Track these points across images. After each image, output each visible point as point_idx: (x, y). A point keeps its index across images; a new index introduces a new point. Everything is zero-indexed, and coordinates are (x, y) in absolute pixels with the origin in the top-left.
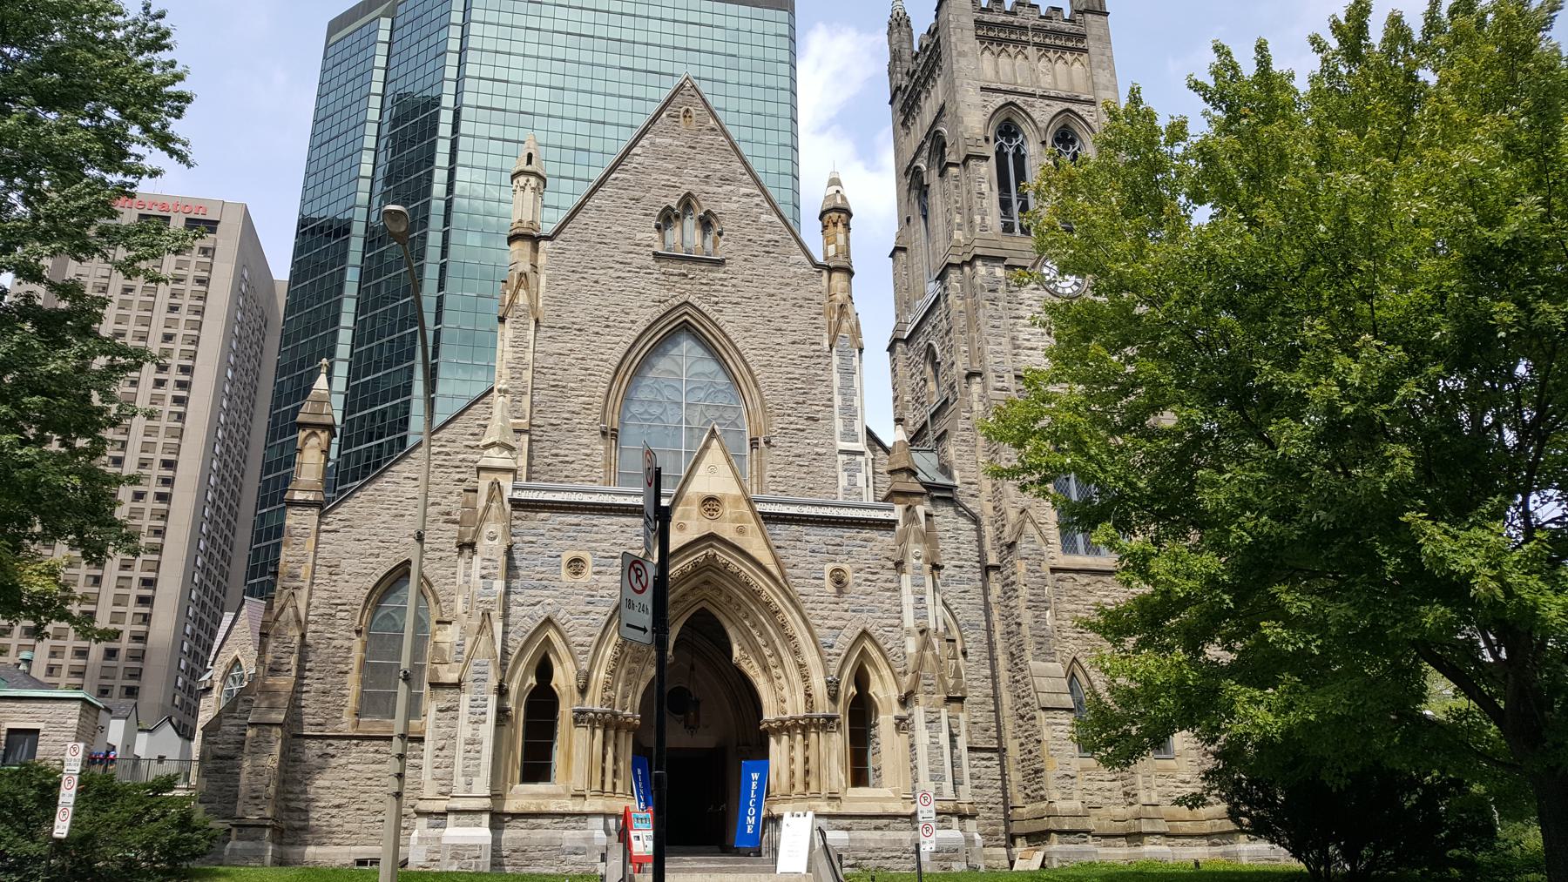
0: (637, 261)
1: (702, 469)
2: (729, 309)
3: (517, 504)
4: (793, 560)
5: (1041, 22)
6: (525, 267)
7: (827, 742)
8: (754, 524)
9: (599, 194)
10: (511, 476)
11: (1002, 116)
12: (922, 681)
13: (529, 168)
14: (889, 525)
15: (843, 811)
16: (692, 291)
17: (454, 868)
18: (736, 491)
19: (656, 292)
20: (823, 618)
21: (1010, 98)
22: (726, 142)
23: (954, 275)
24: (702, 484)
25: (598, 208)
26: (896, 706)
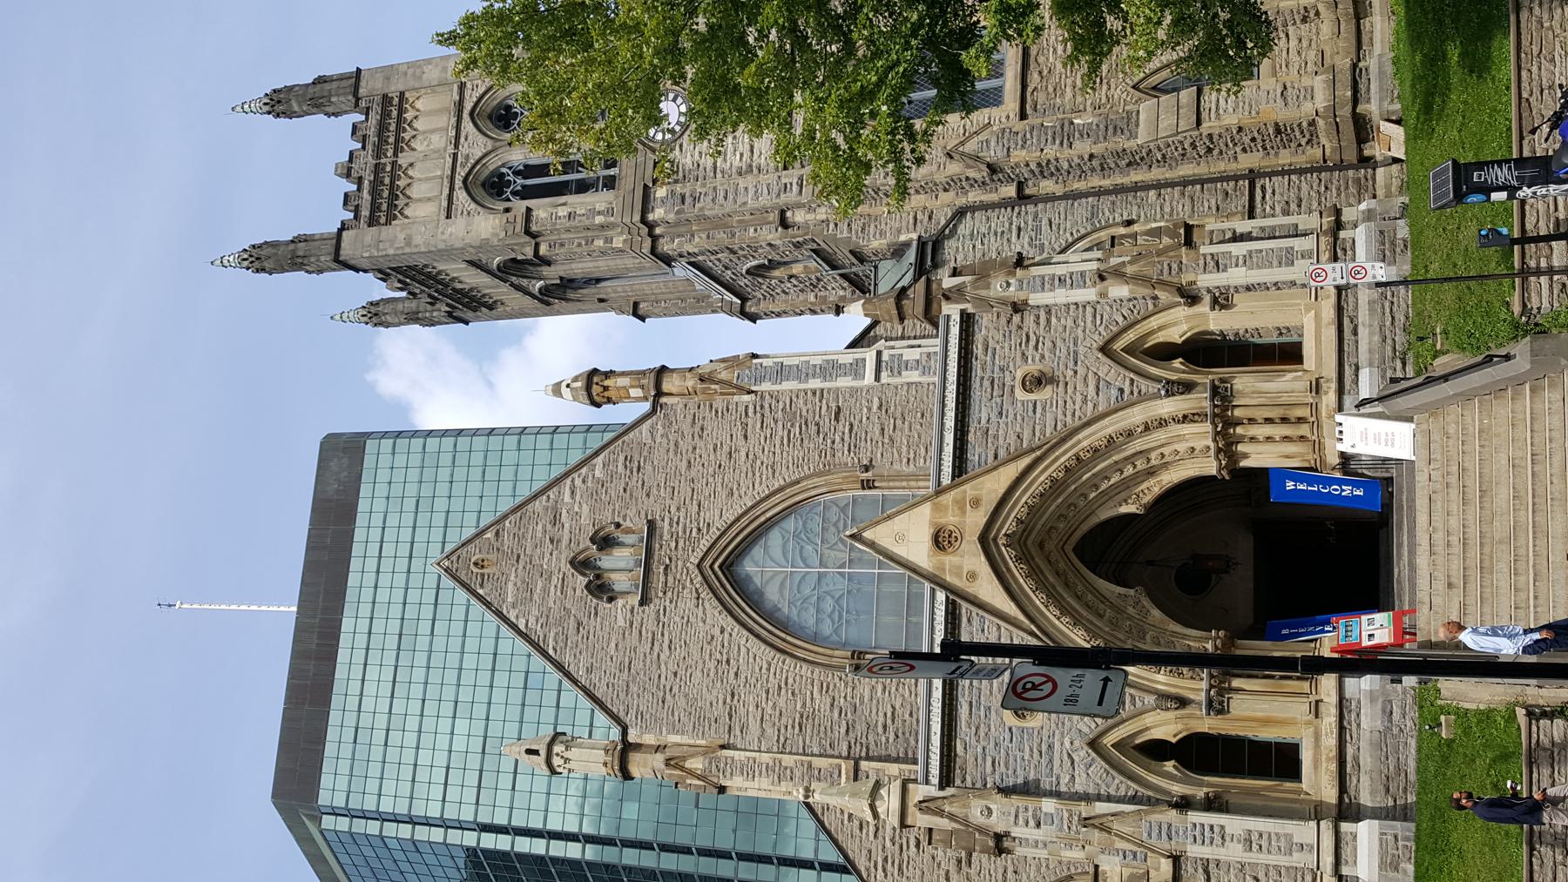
0: (650, 625)
1: (900, 551)
2: (707, 515)
3: (946, 780)
4: (1012, 439)
5: (370, 147)
6: (659, 759)
7: (1243, 394)
8: (967, 487)
9: (572, 669)
10: (911, 786)
11: (479, 193)
12: (1165, 277)
13: (543, 753)
14: (967, 320)
15: (1334, 375)
16: (685, 559)
17: (1411, 868)
18: (926, 508)
19: (687, 603)
20: (1085, 401)
21: (458, 183)
22: (512, 518)
23: (666, 247)
24: (919, 552)
25: (589, 670)
26: (1197, 309)
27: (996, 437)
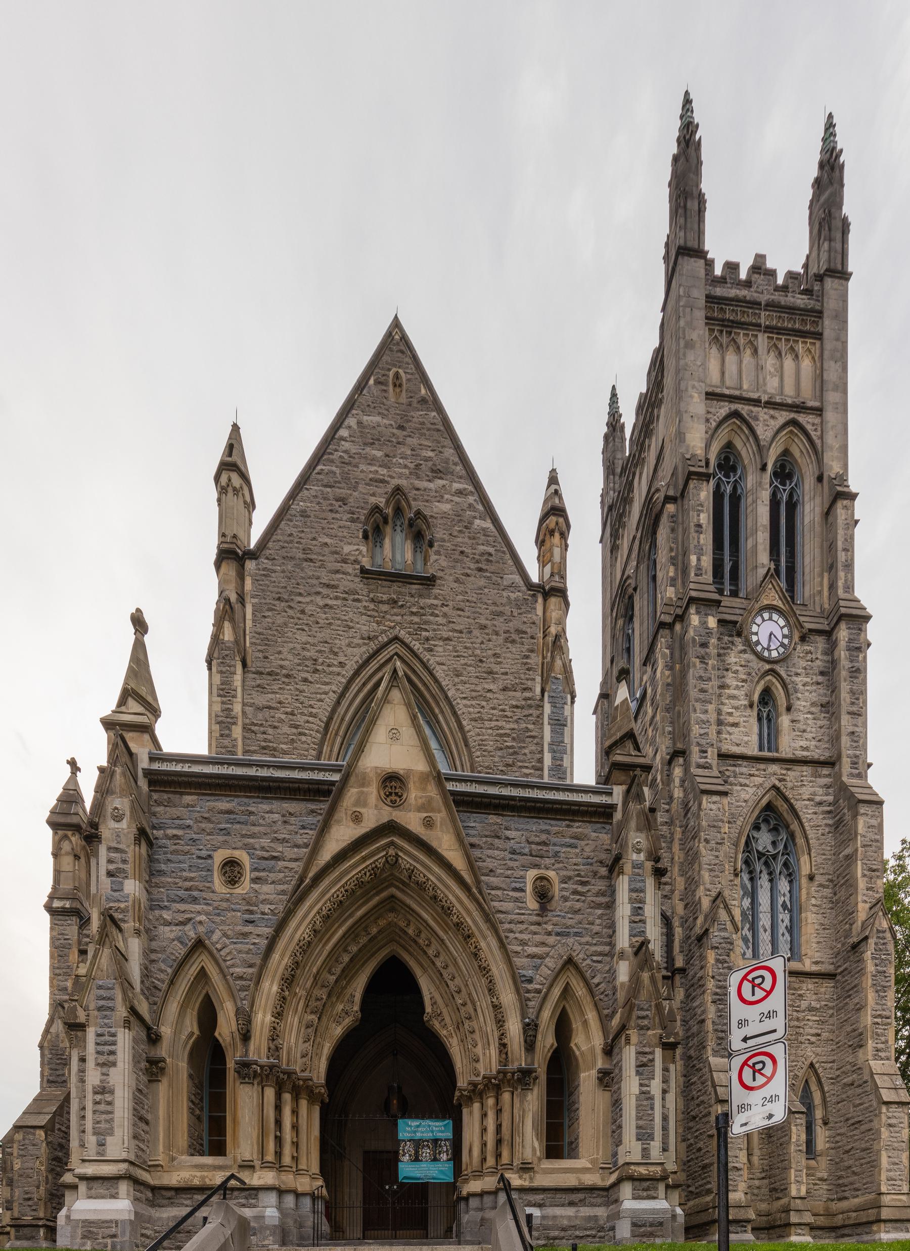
4: (490, 864)
12: (636, 1013)
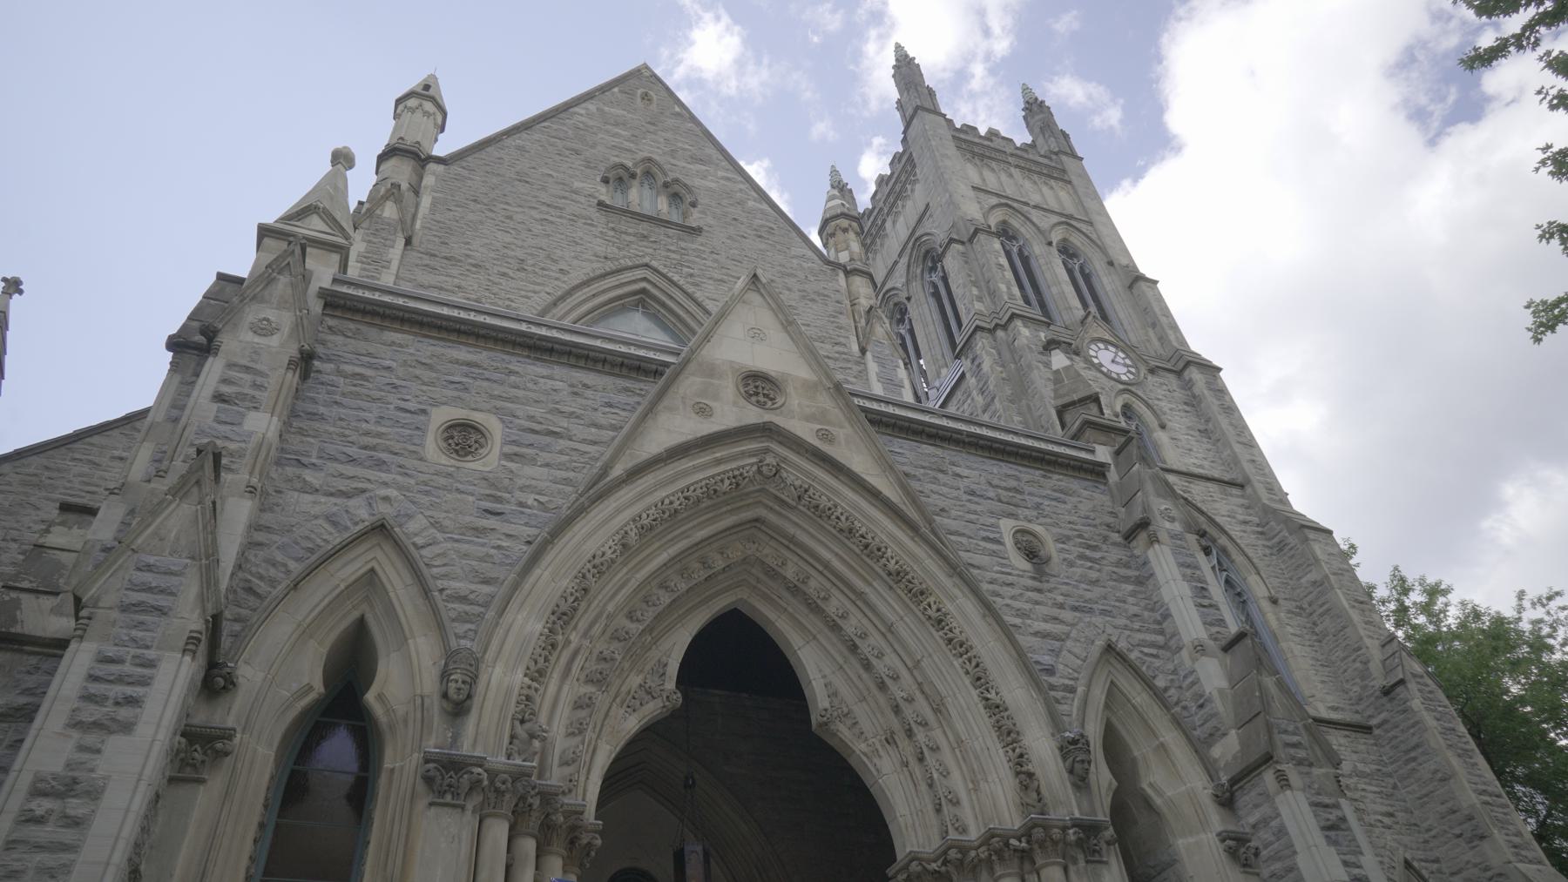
14: (1097, 472)
20: (1021, 614)
27: (935, 481)
